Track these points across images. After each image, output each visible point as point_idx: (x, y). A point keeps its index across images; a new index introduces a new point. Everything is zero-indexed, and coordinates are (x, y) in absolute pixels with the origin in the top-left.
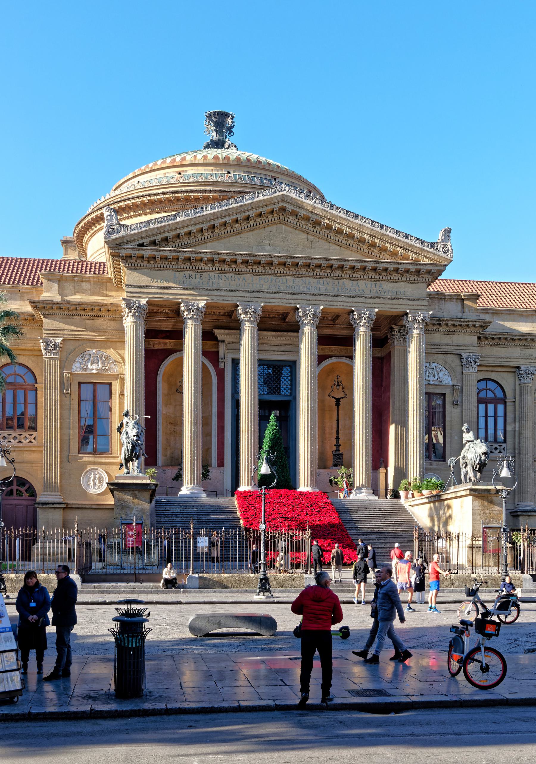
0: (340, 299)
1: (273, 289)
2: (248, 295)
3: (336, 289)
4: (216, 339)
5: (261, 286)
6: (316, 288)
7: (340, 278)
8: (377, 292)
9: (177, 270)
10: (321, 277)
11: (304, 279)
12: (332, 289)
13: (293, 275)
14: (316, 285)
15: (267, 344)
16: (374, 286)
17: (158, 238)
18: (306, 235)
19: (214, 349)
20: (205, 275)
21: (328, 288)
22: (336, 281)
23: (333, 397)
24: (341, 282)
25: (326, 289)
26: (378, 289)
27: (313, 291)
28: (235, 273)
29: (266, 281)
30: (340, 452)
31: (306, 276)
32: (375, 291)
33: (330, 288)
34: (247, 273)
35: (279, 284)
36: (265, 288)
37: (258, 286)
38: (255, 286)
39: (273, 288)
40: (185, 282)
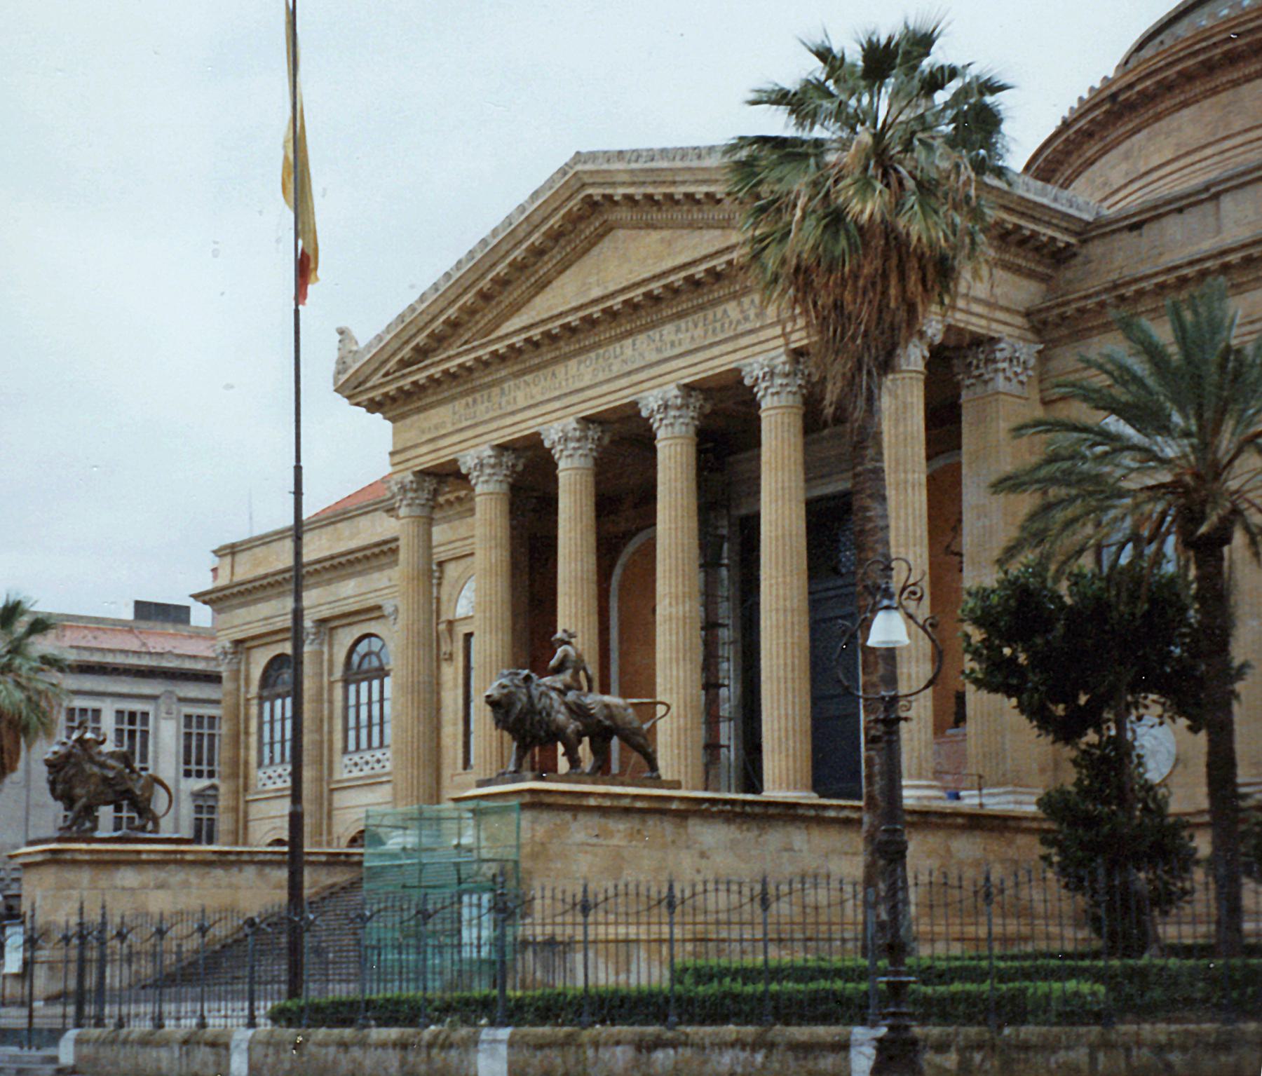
0: (716, 351)
1: (601, 377)
2: (557, 405)
7: (714, 303)
9: (453, 398)
10: (680, 316)
13: (630, 334)
17: (406, 352)
20: (496, 390)
22: (710, 314)
24: (719, 311)
25: (692, 338)
27: (667, 354)
28: (538, 367)
31: (653, 325)
34: (555, 361)
36: (587, 381)
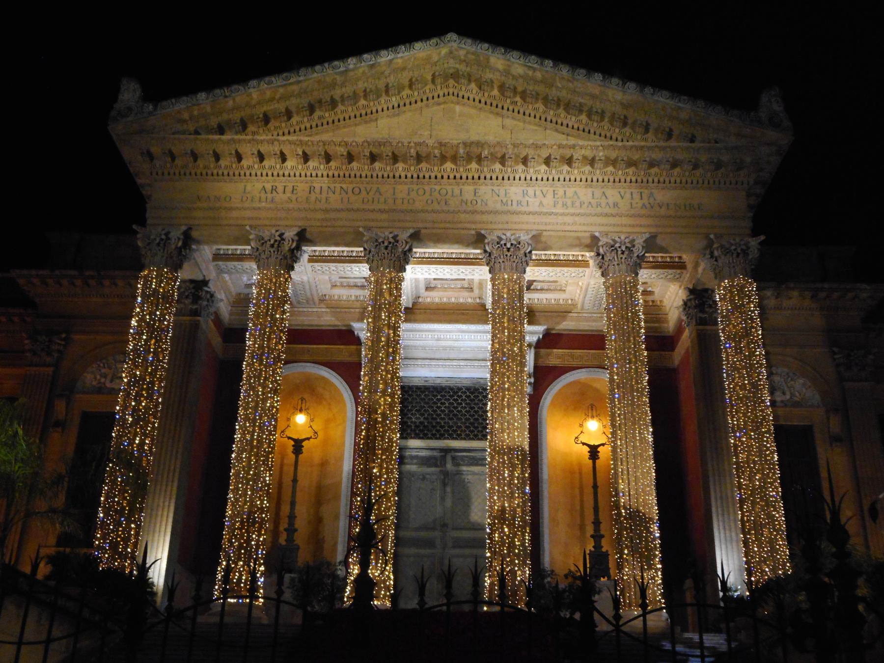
2: (384, 216)
3: (561, 203)
4: (357, 341)
5: (411, 201)
6: (519, 203)
8: (644, 205)
11: (495, 188)
12: (552, 203)
14: (520, 198)
15: (452, 348)
16: (636, 196)
18: (500, 119)
19: (353, 359)
21: (545, 201)
23: (584, 444)
25: (541, 204)
26: (645, 201)
29: (421, 192)
30: (604, 550)
32: (640, 205)
33: (549, 200)
35: (447, 197)
37: (406, 201)
38: (399, 202)
39: (435, 203)
40: (263, 199)
